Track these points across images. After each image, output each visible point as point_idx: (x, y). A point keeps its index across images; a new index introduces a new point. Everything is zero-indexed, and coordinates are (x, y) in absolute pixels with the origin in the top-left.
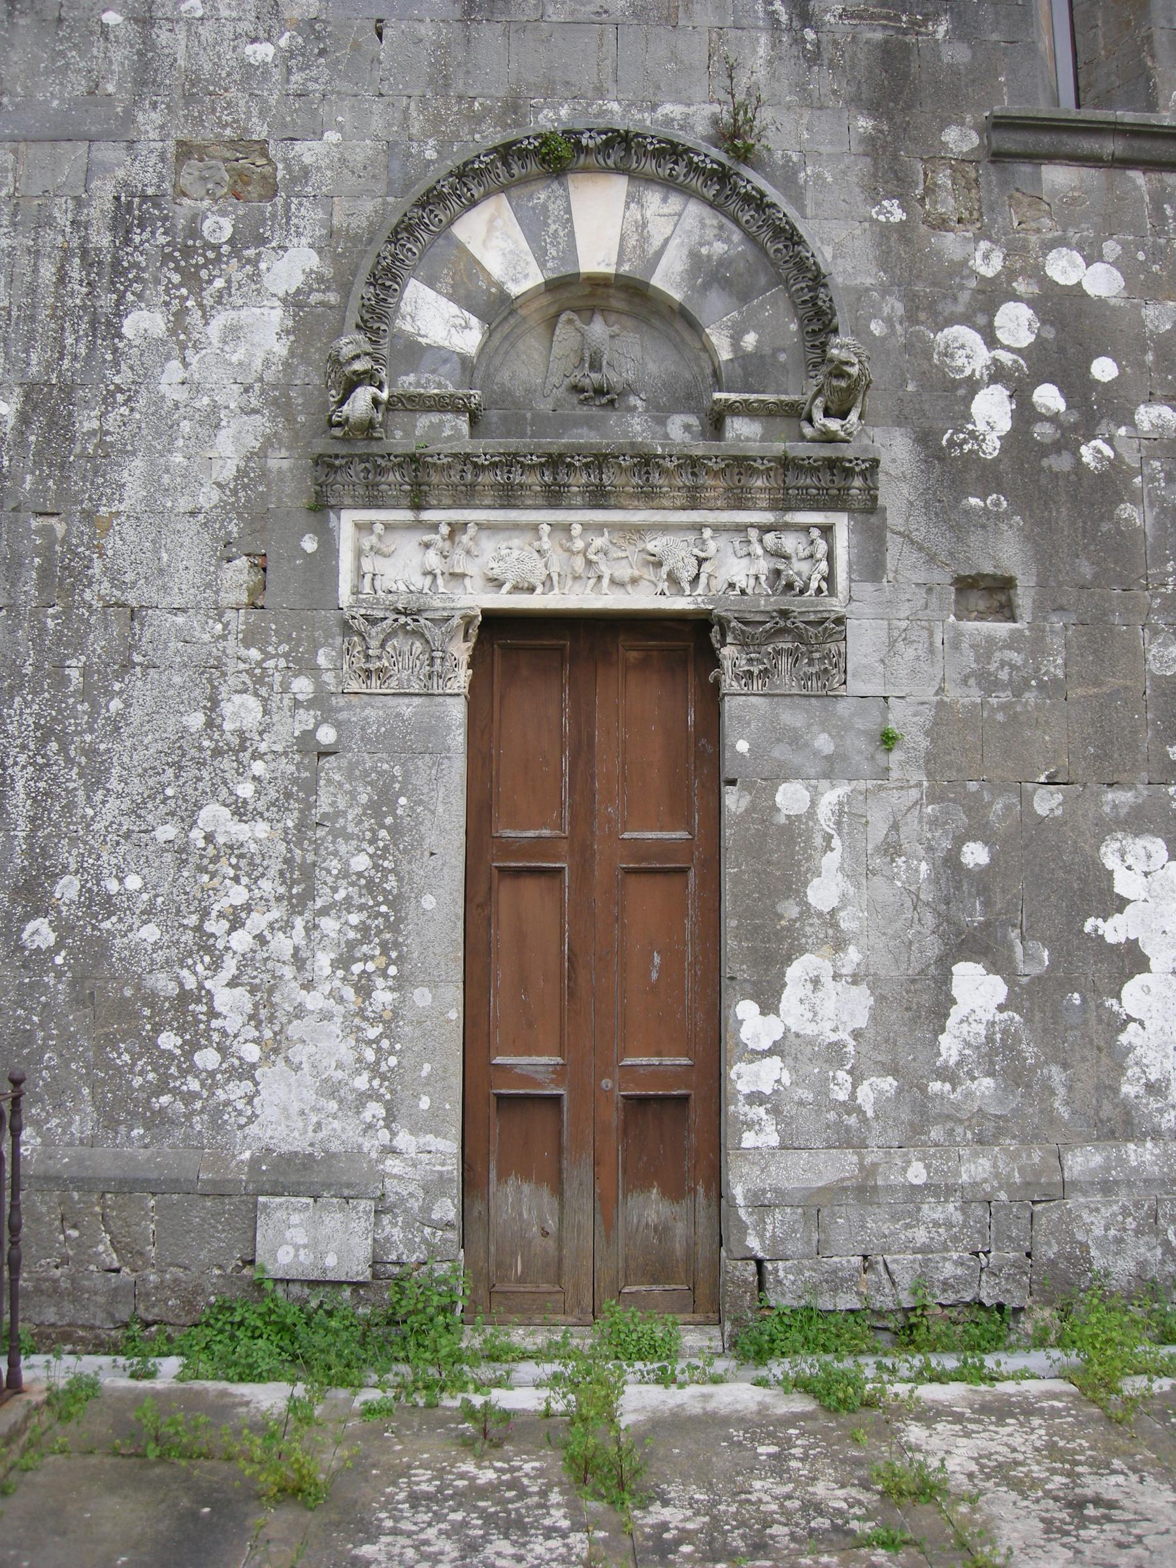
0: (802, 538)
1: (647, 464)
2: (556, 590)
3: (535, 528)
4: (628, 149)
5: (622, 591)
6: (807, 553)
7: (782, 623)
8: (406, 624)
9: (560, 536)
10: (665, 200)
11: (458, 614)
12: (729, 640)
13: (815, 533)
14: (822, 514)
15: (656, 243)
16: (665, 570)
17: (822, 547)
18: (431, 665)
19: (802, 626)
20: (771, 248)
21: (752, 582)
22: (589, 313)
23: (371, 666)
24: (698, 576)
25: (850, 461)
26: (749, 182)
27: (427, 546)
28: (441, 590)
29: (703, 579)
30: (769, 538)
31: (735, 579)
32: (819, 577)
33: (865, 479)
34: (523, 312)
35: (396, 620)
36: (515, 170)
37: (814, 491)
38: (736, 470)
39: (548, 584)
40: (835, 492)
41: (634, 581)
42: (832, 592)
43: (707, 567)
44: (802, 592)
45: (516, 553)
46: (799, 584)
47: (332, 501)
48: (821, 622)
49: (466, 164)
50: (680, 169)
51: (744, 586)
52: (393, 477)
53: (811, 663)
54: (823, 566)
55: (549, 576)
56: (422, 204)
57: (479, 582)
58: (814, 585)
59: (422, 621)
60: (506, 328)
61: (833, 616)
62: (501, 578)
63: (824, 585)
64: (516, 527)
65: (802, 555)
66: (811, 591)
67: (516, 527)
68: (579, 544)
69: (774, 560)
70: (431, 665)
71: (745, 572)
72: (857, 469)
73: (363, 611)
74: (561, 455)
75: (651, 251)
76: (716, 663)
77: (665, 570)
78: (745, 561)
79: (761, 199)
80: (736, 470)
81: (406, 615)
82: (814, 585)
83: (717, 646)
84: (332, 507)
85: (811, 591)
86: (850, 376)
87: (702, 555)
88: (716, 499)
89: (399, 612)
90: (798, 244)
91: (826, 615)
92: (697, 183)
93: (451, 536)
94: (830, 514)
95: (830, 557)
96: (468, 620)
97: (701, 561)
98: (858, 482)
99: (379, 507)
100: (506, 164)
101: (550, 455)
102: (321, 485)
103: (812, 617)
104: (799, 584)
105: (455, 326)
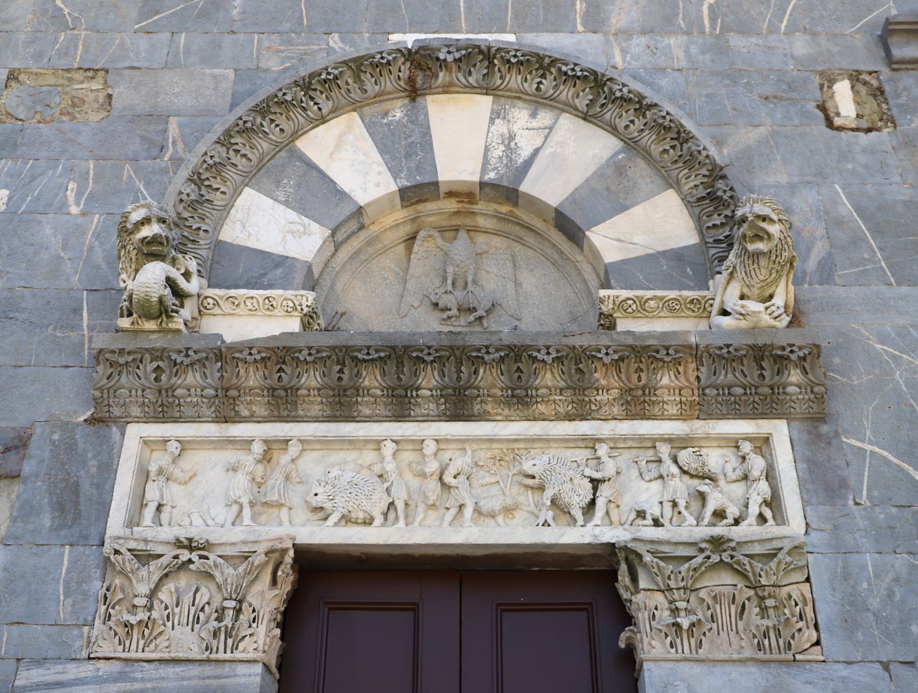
0: (729, 453)
1: (518, 358)
2: (401, 523)
3: (377, 444)
4: (491, 65)
5: (491, 522)
6: (739, 473)
7: (715, 558)
8: (190, 561)
9: (408, 456)
10: (533, 115)
11: (262, 548)
12: (643, 583)
13: (746, 447)
14: (752, 423)
15: (525, 153)
16: (549, 493)
17: (757, 464)
18: (219, 619)
19: (746, 560)
20: (656, 150)
21: (668, 507)
22: (452, 234)
23: (133, 620)
24: (593, 503)
25: (783, 349)
26: (624, 85)
27: (234, 469)
28: (247, 520)
29: (600, 503)
30: (684, 456)
31: (645, 507)
32: (760, 500)
33: (805, 372)
34: (374, 229)
35: (176, 557)
36: (369, 87)
37: (739, 391)
38: (634, 366)
39: (391, 516)
40: (767, 390)
41: (508, 510)
42: (780, 518)
43: (605, 492)
44: (737, 522)
45: (348, 476)
46: (733, 511)
47: (116, 411)
48: (771, 556)
49: (311, 76)
50: (547, 84)
51: (657, 512)
52: (192, 378)
53: (764, 611)
54: (763, 487)
55: (392, 504)
56: (262, 110)
57: (301, 515)
58: (754, 510)
59: (212, 557)
60: (355, 243)
61: (787, 545)
62: (328, 505)
63: (768, 513)
64: (352, 443)
65: (732, 476)
66: (752, 519)
67: (352, 443)
68: (432, 466)
69: (696, 482)
70: (219, 619)
71: (658, 499)
72: (793, 357)
73: (132, 545)
74: (406, 348)
75: (520, 161)
76: (628, 620)
77: (549, 493)
78: (656, 486)
79: (639, 102)
80: (634, 366)
81: (191, 549)
82: (754, 510)
83: (625, 595)
84: (115, 420)
85: (752, 519)
86: (769, 236)
87: (597, 475)
88: (610, 403)
89: (184, 547)
90: (687, 141)
91: (776, 544)
92: (566, 93)
93: (266, 458)
94: (761, 422)
95: (770, 475)
96: (275, 555)
97: (596, 483)
98: (795, 376)
99: (176, 421)
100: (358, 79)
101: (393, 348)
102: (100, 389)
103: (757, 549)
104: (733, 511)
105: (293, 233)
